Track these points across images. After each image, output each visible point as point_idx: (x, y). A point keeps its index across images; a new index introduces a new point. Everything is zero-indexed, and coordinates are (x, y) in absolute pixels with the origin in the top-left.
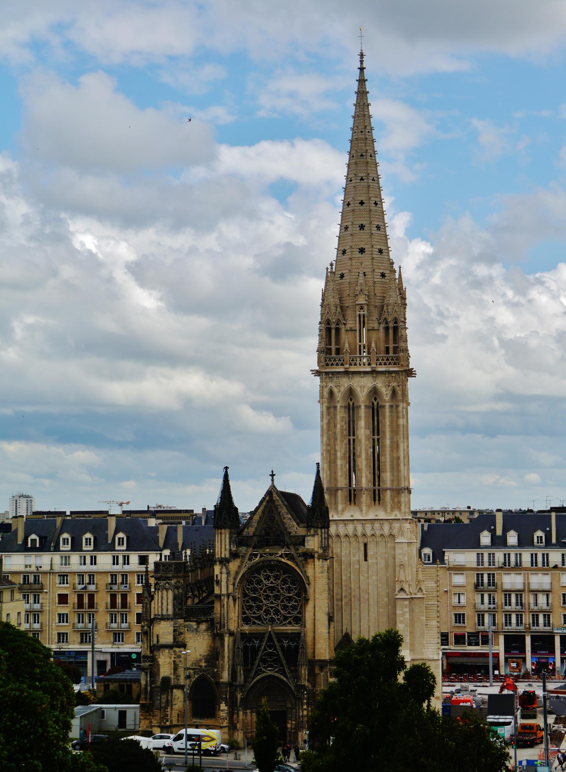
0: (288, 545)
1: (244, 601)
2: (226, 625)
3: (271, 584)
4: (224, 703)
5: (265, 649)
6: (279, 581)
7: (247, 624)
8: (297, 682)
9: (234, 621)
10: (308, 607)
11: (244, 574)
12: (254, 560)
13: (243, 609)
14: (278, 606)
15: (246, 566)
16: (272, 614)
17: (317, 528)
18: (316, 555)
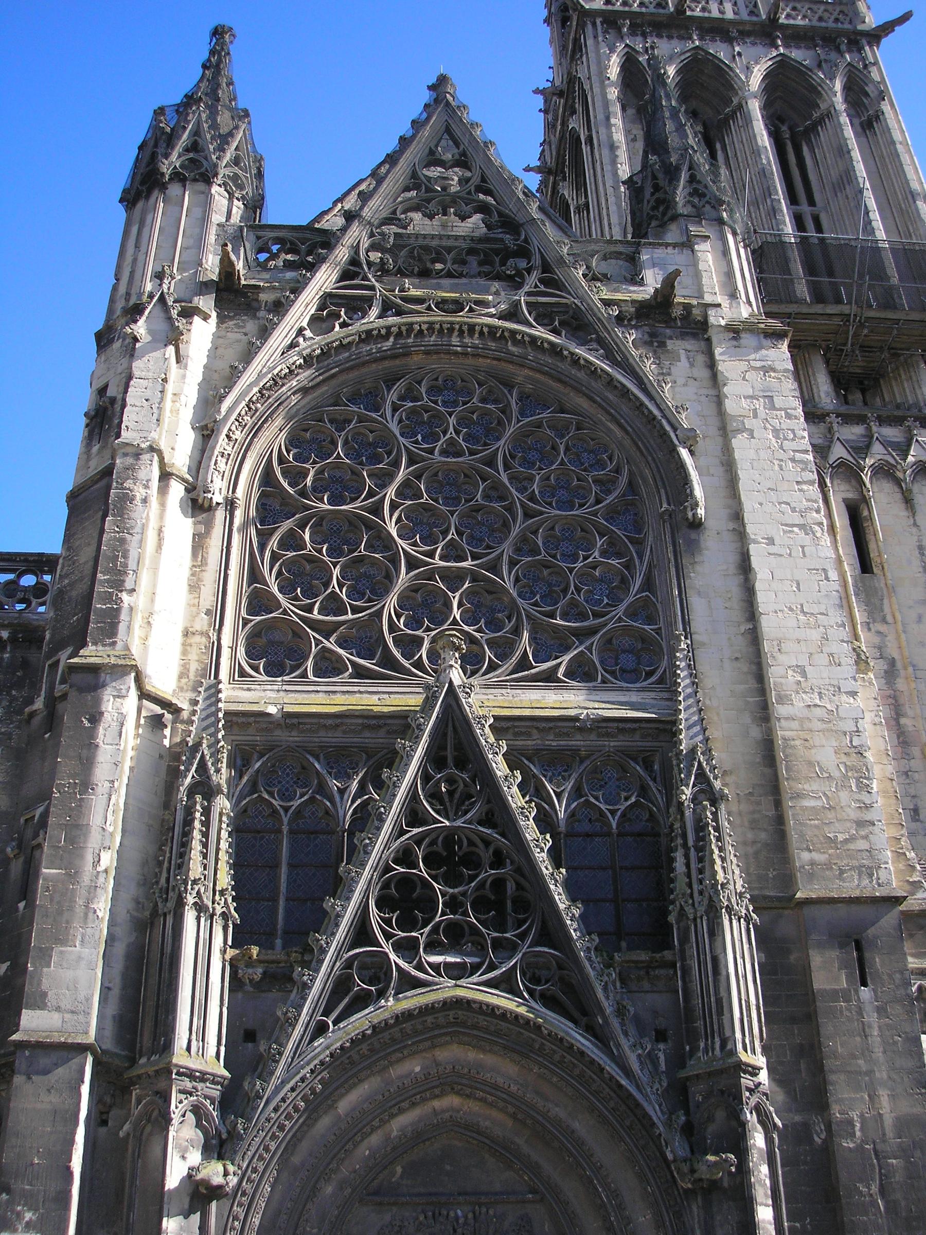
0: (546, 267)
1: (264, 537)
2: (124, 616)
3: (444, 453)
4: (28, 1216)
5: (413, 815)
6: (502, 445)
7: (275, 670)
8: (679, 1060)
9: (186, 634)
10: (698, 568)
11: (277, 382)
12: (344, 325)
13: (254, 575)
14: (494, 567)
15: (292, 346)
16: (456, 613)
17: (698, 217)
18: (717, 319)
